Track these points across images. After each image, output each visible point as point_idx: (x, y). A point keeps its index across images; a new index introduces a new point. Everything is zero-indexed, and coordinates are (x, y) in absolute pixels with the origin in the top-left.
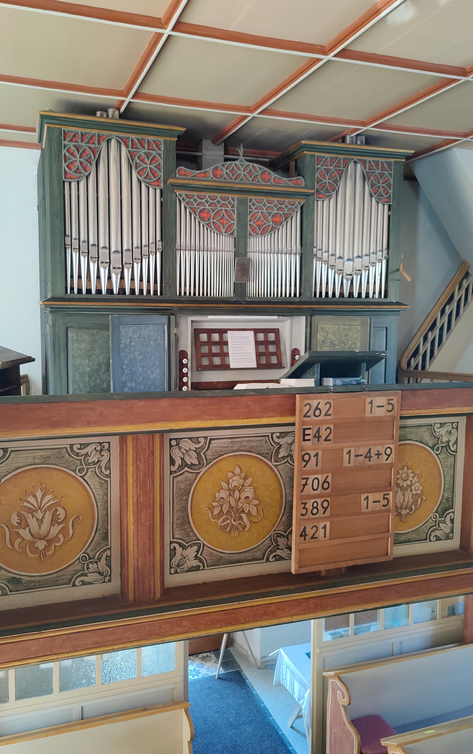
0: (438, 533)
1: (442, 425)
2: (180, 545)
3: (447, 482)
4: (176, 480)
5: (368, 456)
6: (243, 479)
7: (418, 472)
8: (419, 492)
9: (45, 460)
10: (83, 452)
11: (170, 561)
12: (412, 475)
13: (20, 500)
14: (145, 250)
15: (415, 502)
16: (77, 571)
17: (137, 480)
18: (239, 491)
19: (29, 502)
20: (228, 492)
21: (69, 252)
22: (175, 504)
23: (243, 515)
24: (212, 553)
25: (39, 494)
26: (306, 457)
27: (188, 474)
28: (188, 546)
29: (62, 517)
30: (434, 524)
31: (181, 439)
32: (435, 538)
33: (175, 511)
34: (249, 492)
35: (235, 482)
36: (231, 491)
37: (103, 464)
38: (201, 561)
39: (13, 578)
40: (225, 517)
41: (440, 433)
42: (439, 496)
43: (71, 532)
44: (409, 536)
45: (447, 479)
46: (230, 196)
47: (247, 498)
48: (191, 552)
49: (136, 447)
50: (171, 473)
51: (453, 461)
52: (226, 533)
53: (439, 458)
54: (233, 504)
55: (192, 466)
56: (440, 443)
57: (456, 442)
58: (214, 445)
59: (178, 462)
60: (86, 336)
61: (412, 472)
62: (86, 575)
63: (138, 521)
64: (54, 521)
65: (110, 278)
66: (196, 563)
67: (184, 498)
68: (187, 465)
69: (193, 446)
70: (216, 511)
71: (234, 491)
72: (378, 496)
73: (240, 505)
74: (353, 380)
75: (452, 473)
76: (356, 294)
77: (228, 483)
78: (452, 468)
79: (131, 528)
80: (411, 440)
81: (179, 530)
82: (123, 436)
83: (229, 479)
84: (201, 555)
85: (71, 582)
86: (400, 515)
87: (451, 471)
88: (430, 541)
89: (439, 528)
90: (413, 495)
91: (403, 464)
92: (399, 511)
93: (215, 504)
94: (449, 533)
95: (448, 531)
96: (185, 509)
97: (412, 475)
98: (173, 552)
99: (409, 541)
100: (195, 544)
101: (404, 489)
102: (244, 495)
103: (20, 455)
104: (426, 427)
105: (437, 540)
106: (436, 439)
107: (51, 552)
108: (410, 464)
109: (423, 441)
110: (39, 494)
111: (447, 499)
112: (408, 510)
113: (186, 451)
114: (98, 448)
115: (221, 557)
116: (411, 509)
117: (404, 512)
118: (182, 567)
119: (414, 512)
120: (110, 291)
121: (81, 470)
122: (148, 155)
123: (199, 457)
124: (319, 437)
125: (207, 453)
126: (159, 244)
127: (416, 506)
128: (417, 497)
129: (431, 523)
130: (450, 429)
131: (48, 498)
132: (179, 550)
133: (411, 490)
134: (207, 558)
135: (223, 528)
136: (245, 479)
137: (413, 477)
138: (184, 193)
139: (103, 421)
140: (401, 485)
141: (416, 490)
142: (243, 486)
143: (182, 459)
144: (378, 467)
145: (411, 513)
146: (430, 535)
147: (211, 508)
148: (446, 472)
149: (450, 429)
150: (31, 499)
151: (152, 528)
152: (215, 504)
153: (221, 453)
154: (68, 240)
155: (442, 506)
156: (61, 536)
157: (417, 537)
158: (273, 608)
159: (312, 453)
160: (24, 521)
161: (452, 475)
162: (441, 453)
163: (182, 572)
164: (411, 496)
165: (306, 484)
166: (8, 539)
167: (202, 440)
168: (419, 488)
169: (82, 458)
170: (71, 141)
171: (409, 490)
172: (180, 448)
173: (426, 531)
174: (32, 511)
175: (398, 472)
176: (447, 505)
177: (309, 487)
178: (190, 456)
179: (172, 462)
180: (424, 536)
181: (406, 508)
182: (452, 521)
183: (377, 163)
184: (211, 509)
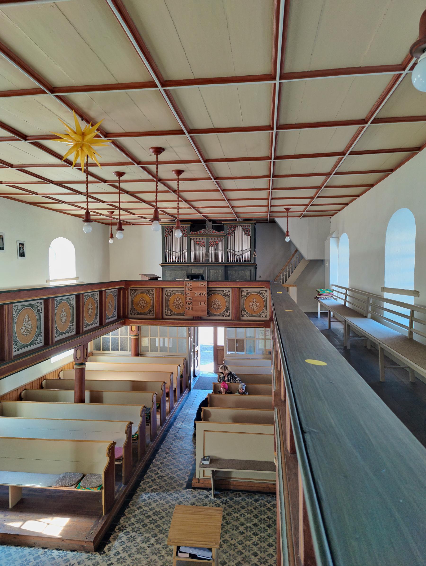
0: (225, 315)
1: (226, 291)
2: (167, 310)
5: (200, 294)
14: (183, 252)
15: (219, 307)
21: (166, 253)
25: (142, 298)
26: (187, 294)
27: (168, 296)
34: (181, 301)
35: (178, 299)
36: (177, 301)
37: (153, 293)
38: (171, 314)
44: (218, 315)
46: (204, 237)
48: (169, 312)
49: (157, 290)
54: (177, 303)
55: (169, 295)
57: (229, 295)
59: (166, 294)
60: (169, 272)
63: (157, 304)
64: (145, 303)
65: (175, 258)
66: (170, 314)
69: (169, 291)
70: (174, 304)
72: (203, 303)
74: (198, 279)
79: (156, 305)
82: (155, 288)
85: (147, 314)
86: (215, 310)
96: (168, 303)
98: (166, 312)
99: (218, 316)
102: (180, 302)
110: (142, 298)
111: (228, 307)
116: (218, 309)
117: (217, 309)
120: (173, 262)
122: (183, 230)
123: (170, 294)
124: (189, 290)
126: (187, 250)
131: (143, 299)
132: (167, 311)
136: (180, 299)
138: (192, 238)
139: (150, 285)
144: (203, 297)
150: (141, 299)
151: (160, 305)
154: (166, 250)
158: (181, 323)
159: (188, 293)
165: (187, 299)
167: (171, 290)
170: (167, 228)
174: (141, 301)
177: (187, 299)
179: (165, 294)
181: (217, 308)
182: (229, 313)
183: (245, 226)
184: (173, 304)
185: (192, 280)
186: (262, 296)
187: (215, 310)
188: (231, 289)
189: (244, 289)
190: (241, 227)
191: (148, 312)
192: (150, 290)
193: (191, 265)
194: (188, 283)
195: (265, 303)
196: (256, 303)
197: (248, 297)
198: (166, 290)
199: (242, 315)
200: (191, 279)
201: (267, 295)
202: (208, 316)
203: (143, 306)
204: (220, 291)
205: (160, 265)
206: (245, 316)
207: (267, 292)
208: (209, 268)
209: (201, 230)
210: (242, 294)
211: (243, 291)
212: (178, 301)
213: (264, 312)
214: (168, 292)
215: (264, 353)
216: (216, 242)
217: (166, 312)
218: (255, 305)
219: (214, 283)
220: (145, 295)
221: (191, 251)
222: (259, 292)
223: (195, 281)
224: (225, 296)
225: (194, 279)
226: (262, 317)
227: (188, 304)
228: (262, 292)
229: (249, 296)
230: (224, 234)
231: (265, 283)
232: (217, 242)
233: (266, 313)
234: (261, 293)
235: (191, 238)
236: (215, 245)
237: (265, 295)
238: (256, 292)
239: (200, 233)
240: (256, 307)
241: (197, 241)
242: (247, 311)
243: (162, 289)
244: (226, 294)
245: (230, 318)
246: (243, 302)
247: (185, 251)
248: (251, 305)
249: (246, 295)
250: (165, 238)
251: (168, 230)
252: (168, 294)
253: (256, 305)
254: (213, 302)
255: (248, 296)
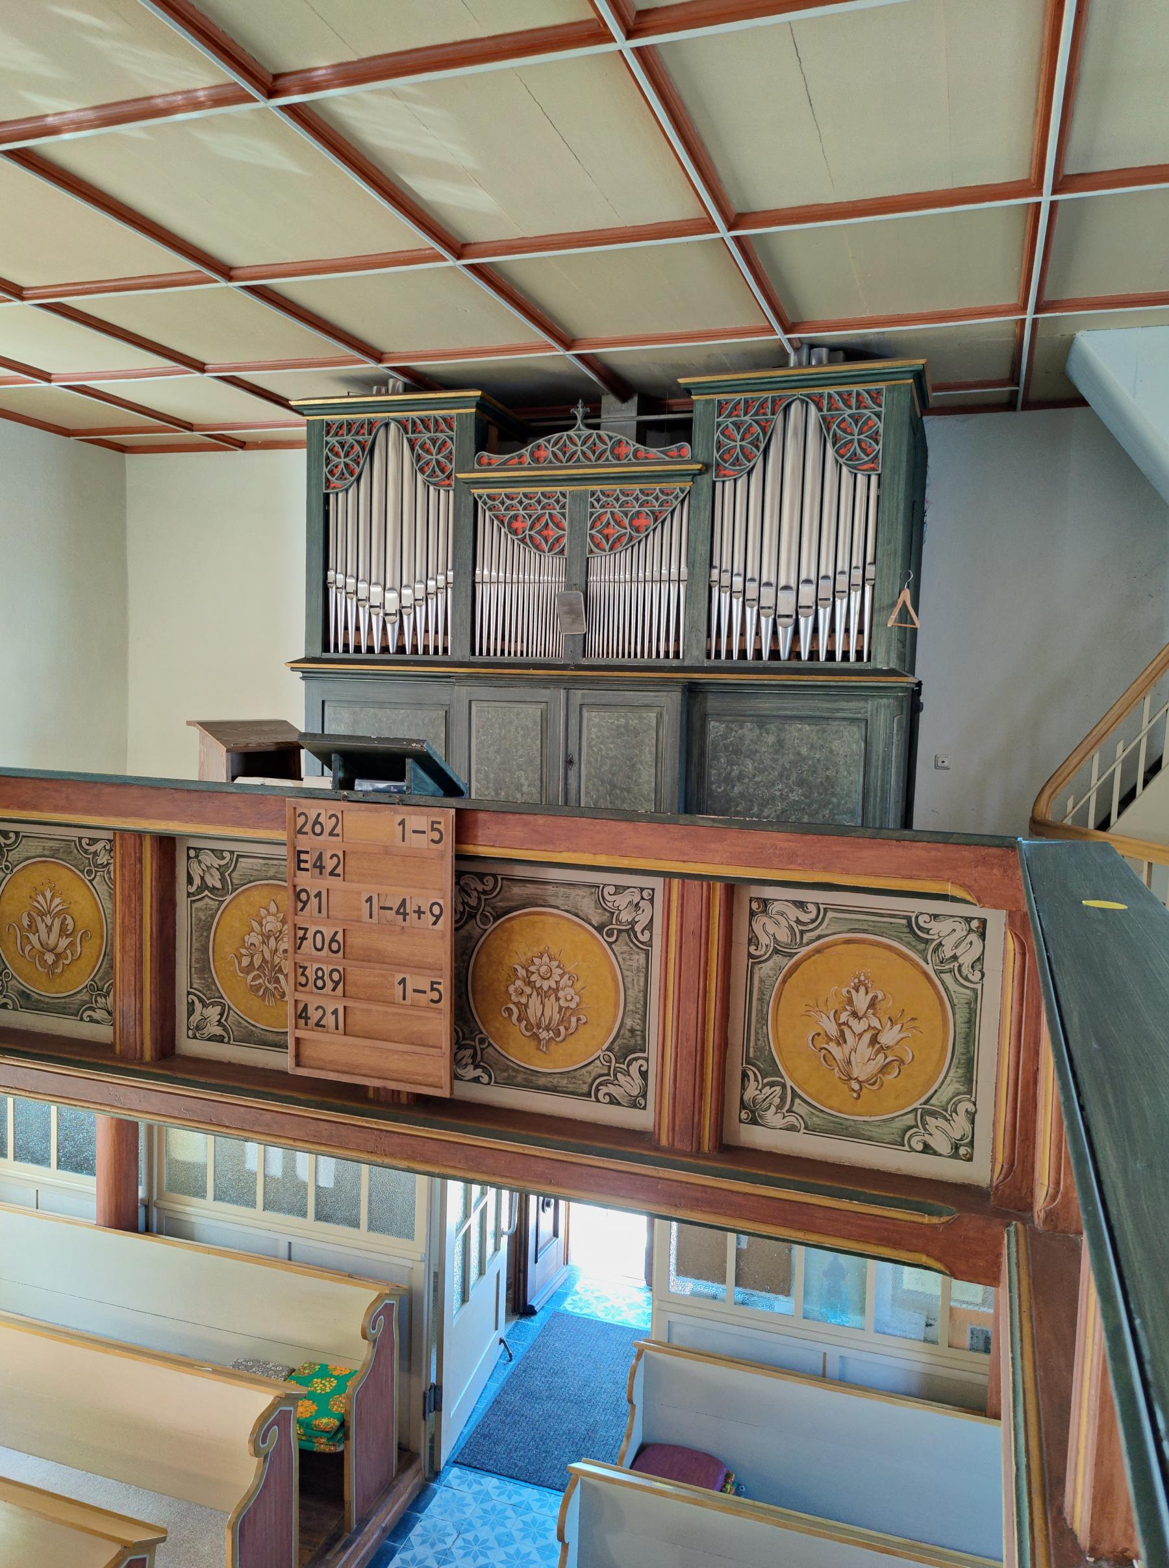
0: (612, 1089)
1: (619, 889)
2: (201, 1000)
3: (630, 999)
4: (194, 906)
6: (281, 921)
7: (570, 968)
8: (573, 1005)
9: (54, 853)
10: (92, 849)
11: (188, 1019)
12: (560, 971)
13: (31, 897)
16: (85, 1002)
17: (122, 893)
18: (276, 938)
19: (38, 902)
20: (260, 937)
22: (194, 940)
23: (281, 977)
24: (240, 1023)
25: (48, 895)
28: (211, 1004)
29: (70, 928)
30: (606, 1071)
31: (201, 849)
32: (607, 1098)
33: (193, 950)
35: (271, 924)
36: (266, 937)
38: (225, 1030)
39: (24, 992)
40: (256, 973)
41: (616, 904)
42: (614, 1022)
43: (79, 949)
45: (630, 993)
47: (285, 951)
48: (213, 1013)
50: (189, 895)
51: (642, 961)
52: (258, 997)
53: (613, 950)
54: (268, 956)
55: (213, 889)
56: (614, 922)
57: (649, 926)
58: (243, 864)
59: (197, 881)
61: (558, 966)
62: (93, 1009)
64: (63, 931)
66: (218, 1031)
67: (205, 934)
68: (207, 887)
69: (217, 862)
70: (245, 962)
71: (269, 937)
73: (277, 960)
75: (642, 984)
76: (805, 650)
77: (261, 924)
78: (642, 975)
80: (557, 907)
81: (200, 978)
83: (262, 918)
84: (226, 1020)
85: (76, 1013)
86: (535, 1036)
87: (638, 980)
88: (598, 1101)
89: (616, 1082)
90: (561, 1008)
91: (542, 948)
92: (534, 1030)
93: (243, 951)
94: (637, 1097)
95: (635, 1092)
96: (204, 949)
97: (561, 972)
99: (554, 1090)
100: (219, 1004)
101: (543, 994)
103: (31, 842)
104: (587, 889)
105: (611, 1103)
106: (608, 914)
107: (59, 970)
108: (554, 950)
109: (581, 914)
110: (48, 895)
111: (632, 1031)
112: (551, 1034)
113: (207, 867)
114: (108, 847)
115: (252, 1031)
116: (559, 1034)
117: (544, 1035)
118: (203, 1032)
119: (564, 1040)
121: (89, 872)
123: (223, 880)
125: (234, 875)
127: (567, 1029)
128: (568, 1014)
129: (598, 1068)
130: (637, 899)
131: (57, 901)
132: (198, 1005)
133: (558, 999)
134: (233, 1027)
135: (255, 989)
137: (562, 976)
140: (538, 985)
141: (566, 1000)
142: (281, 932)
143: (202, 878)
145: (558, 1039)
146: (597, 1090)
147: (238, 955)
148: (630, 979)
149: (637, 899)
150: (40, 898)
152: (243, 951)
153: (252, 879)
155: (619, 1041)
156: (68, 951)
157: (571, 1087)
160: (34, 924)
161: (642, 988)
162: (618, 943)
163: (202, 1039)
164: (556, 1009)
166: (19, 942)
168: (572, 998)
169: (91, 857)
171: (553, 997)
172: (200, 862)
173: (590, 1080)
174: (42, 914)
175: (532, 961)
176: (632, 1042)
178: (212, 875)
179: (190, 880)
180: (585, 1088)
181: (548, 1029)
182: (644, 1075)
184: (239, 957)
185: (351, 787)
186: (929, 969)
187: (533, 1043)
188: (657, 883)
189: (768, 892)
190: (813, 408)
191: (86, 998)
192: (93, 841)
193: (470, 676)
194: (313, 816)
195: (962, 1028)
196: (875, 1023)
197: (807, 957)
198: (198, 850)
199: (743, 1105)
200: (346, 784)
201: (980, 959)
202: (476, 1080)
203: (51, 951)
204: (573, 892)
205: (295, 665)
206: (772, 1117)
207: (983, 936)
208: (578, 695)
209: (541, 441)
210: (757, 927)
211: (765, 902)
212: (272, 940)
213: (945, 1113)
214: (206, 870)
215: (940, 1330)
216: (636, 523)
217: (191, 1011)
218: (867, 1038)
219: (514, 828)
220: (64, 877)
221: (478, 579)
222: (913, 930)
223: (366, 800)
224: (610, 934)
225: (362, 785)
226: (927, 1149)
227: (312, 977)
228: (936, 927)
229: (818, 951)
230: (693, 460)
231: (967, 853)
232: (641, 522)
233: (961, 1121)
234: (927, 941)
235: (476, 492)
236: (631, 539)
237: (966, 960)
238: (878, 923)
239: (537, 460)
240: (869, 1052)
241: (515, 517)
242: (789, 1083)
243: (166, 845)
244: (625, 916)
245: (642, 1119)
246: (760, 1000)
247: (441, 578)
248: (833, 1030)
249: (787, 946)
250: (327, 496)
251: (342, 445)
252: (210, 882)
253: (874, 1041)
254: (522, 972)
255: (804, 951)
